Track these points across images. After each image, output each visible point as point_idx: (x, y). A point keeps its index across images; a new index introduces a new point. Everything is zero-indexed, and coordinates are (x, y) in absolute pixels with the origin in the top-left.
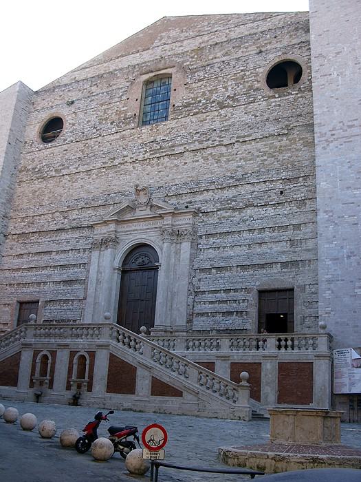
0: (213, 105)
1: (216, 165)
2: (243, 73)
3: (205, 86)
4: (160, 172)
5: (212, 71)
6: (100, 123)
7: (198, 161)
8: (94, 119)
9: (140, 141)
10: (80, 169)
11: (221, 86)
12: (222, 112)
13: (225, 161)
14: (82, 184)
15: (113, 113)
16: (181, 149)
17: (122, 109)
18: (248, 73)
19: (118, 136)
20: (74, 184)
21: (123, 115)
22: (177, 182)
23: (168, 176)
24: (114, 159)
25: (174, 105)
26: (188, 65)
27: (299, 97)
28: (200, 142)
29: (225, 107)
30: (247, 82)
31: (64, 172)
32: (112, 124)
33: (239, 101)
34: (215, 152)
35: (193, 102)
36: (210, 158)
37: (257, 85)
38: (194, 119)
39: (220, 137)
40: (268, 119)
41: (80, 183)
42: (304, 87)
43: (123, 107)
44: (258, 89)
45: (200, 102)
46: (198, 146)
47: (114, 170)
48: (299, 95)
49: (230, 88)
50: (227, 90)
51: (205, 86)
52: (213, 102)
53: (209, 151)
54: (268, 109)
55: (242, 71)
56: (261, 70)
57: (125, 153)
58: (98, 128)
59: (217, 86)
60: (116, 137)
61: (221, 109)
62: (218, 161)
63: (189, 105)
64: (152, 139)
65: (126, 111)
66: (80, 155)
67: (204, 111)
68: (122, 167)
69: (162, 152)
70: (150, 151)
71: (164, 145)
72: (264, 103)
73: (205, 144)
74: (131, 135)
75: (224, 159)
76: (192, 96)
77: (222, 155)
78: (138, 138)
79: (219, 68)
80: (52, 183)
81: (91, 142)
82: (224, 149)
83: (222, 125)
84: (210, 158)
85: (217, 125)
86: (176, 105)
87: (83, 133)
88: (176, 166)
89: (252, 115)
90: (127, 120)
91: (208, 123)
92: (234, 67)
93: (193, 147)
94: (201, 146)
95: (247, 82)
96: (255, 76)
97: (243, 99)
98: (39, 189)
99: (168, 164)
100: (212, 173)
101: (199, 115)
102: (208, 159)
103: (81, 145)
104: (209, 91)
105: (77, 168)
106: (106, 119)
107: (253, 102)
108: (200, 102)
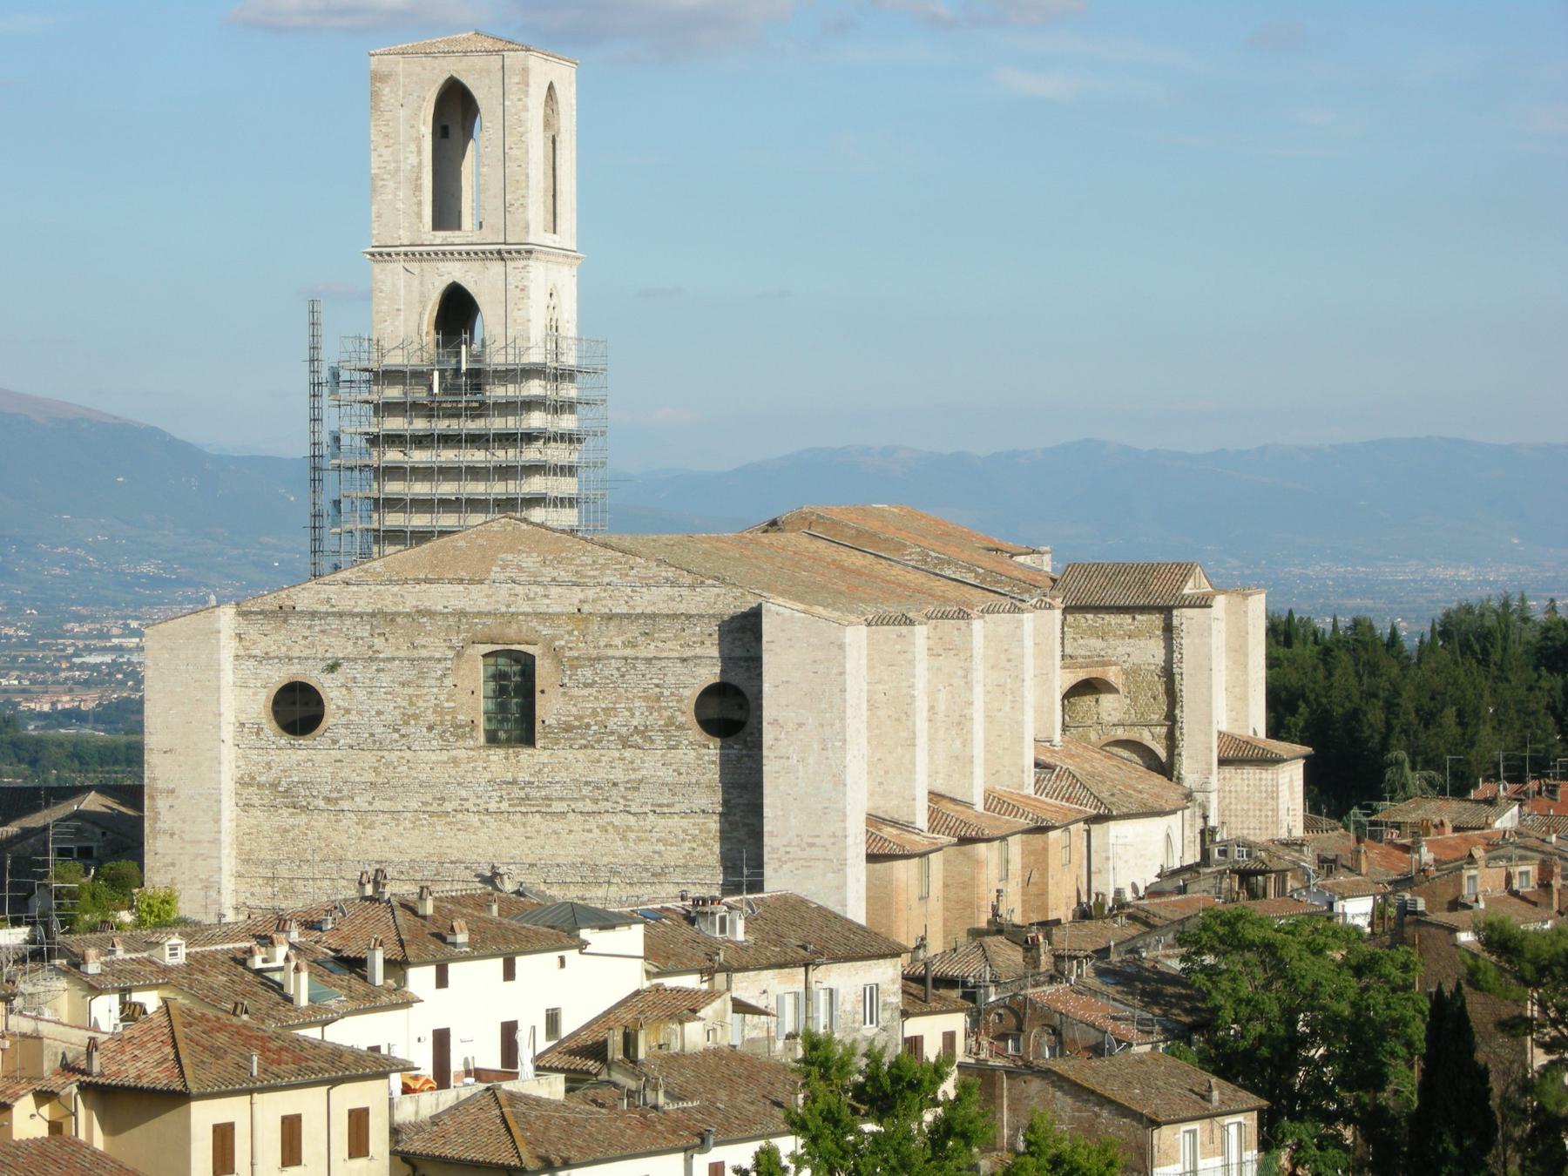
0: (611, 738)
1: (620, 843)
2: (658, 690)
3: (596, 698)
4: (527, 838)
5: (606, 673)
6: (406, 723)
7: (590, 831)
8: (392, 716)
9: (488, 776)
10: (378, 805)
11: (623, 705)
12: (628, 753)
13: (634, 840)
14: (384, 833)
15: (427, 708)
16: (558, 807)
17: (446, 705)
18: (666, 693)
19: (444, 756)
20: (368, 831)
21: (448, 718)
22: (559, 860)
23: (543, 848)
24: (443, 799)
25: (543, 722)
26: (562, 648)
27: (743, 756)
28: (596, 801)
29: (630, 746)
30: (666, 708)
31: (345, 805)
32: (430, 728)
33: (652, 741)
34: (617, 820)
35: (576, 723)
36: (610, 828)
37: (681, 719)
38: (580, 755)
39: (624, 797)
40: (697, 783)
41: (379, 832)
42: (752, 741)
43: (447, 701)
44: (680, 727)
45: (588, 726)
46: (590, 807)
47: (444, 820)
48: (744, 752)
49: (637, 714)
50: (633, 715)
51: (596, 698)
52: (612, 733)
53: (607, 818)
54: (699, 765)
55: (657, 686)
56: (687, 692)
57: (464, 793)
58: (403, 732)
59: (615, 703)
60: (440, 758)
61: (624, 748)
62: (624, 838)
63: (568, 728)
64: (509, 776)
65: (454, 711)
66: (371, 777)
67: (596, 746)
68: (460, 816)
69: (530, 805)
70: (509, 800)
71: (533, 793)
72: (693, 753)
73: (603, 805)
74: (470, 760)
75: (632, 836)
76: (574, 711)
77: (629, 828)
78: (485, 768)
79: (618, 669)
80: (320, 822)
81: (392, 757)
82: (632, 820)
83: (627, 778)
84: (610, 828)
85: (618, 775)
86: (547, 723)
87: (372, 735)
88: (555, 832)
89: (674, 771)
90: (461, 731)
91: (604, 768)
92: (643, 675)
93: (579, 806)
94: (595, 808)
95: (666, 708)
96: (678, 701)
97: (659, 739)
98: (293, 827)
99: (543, 827)
100: (615, 856)
101: (589, 751)
102: (606, 831)
103: (370, 757)
104: (603, 709)
105: (370, 804)
106: (416, 717)
107: (675, 748)
108: (588, 726)
